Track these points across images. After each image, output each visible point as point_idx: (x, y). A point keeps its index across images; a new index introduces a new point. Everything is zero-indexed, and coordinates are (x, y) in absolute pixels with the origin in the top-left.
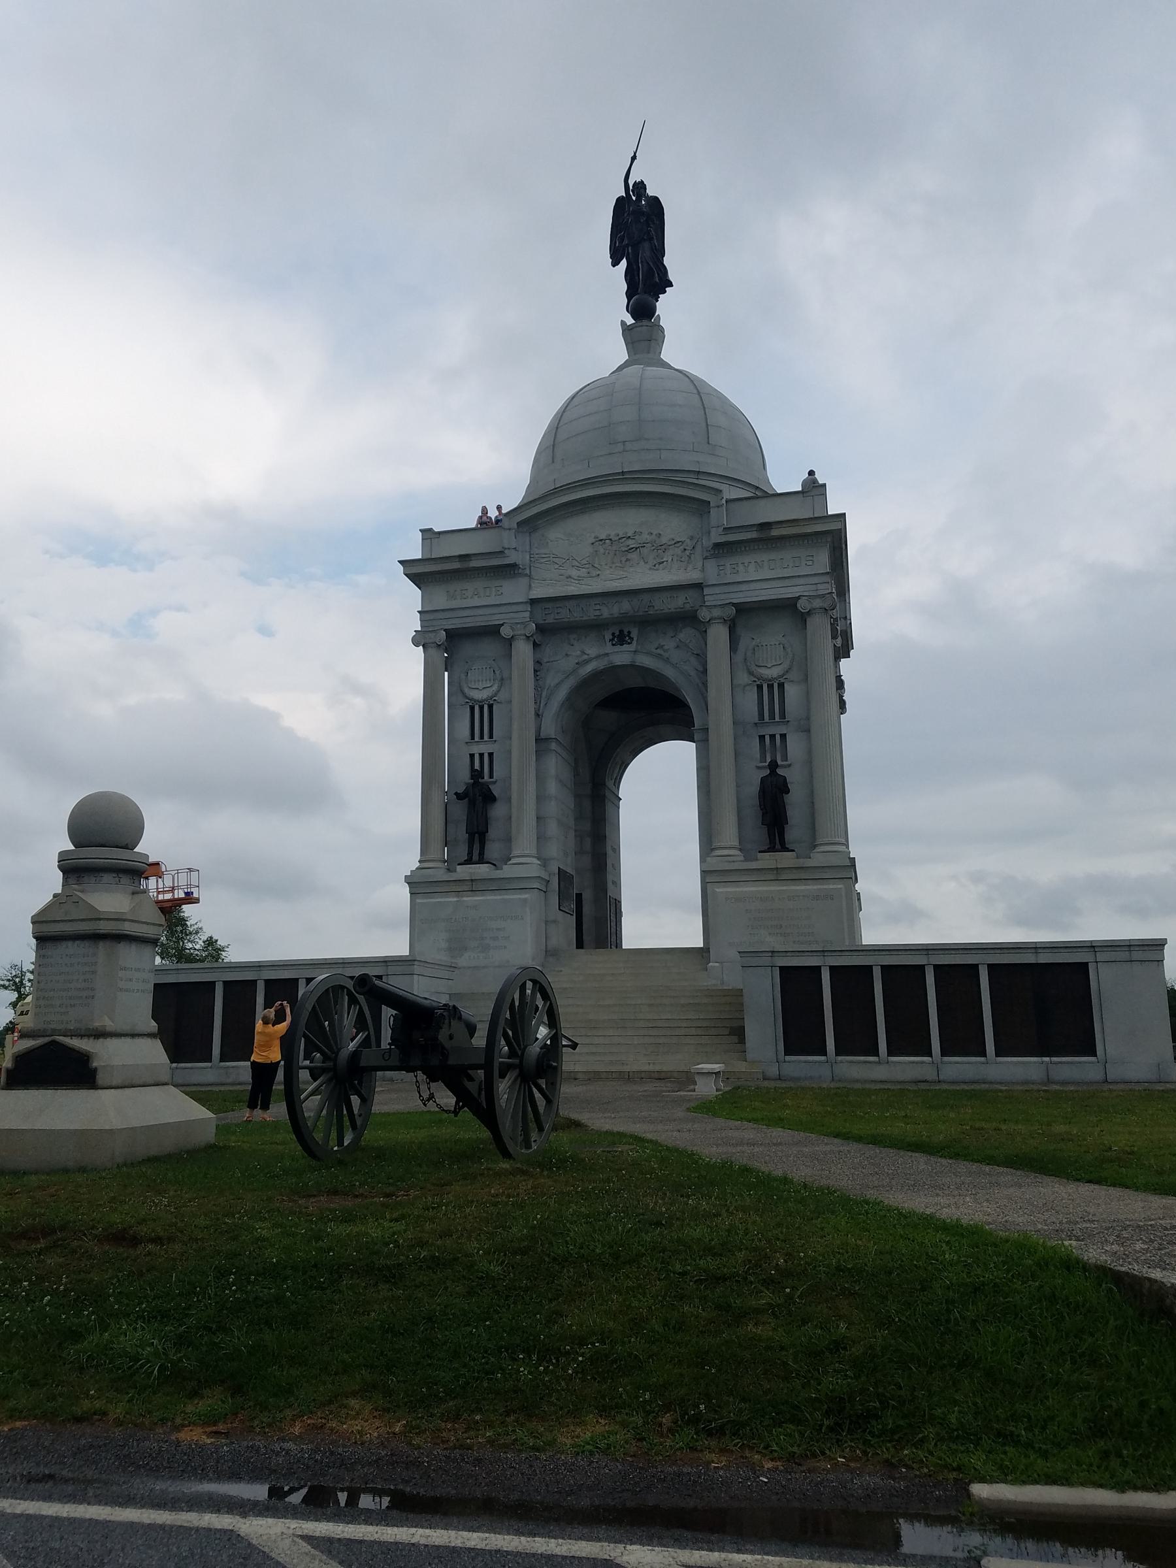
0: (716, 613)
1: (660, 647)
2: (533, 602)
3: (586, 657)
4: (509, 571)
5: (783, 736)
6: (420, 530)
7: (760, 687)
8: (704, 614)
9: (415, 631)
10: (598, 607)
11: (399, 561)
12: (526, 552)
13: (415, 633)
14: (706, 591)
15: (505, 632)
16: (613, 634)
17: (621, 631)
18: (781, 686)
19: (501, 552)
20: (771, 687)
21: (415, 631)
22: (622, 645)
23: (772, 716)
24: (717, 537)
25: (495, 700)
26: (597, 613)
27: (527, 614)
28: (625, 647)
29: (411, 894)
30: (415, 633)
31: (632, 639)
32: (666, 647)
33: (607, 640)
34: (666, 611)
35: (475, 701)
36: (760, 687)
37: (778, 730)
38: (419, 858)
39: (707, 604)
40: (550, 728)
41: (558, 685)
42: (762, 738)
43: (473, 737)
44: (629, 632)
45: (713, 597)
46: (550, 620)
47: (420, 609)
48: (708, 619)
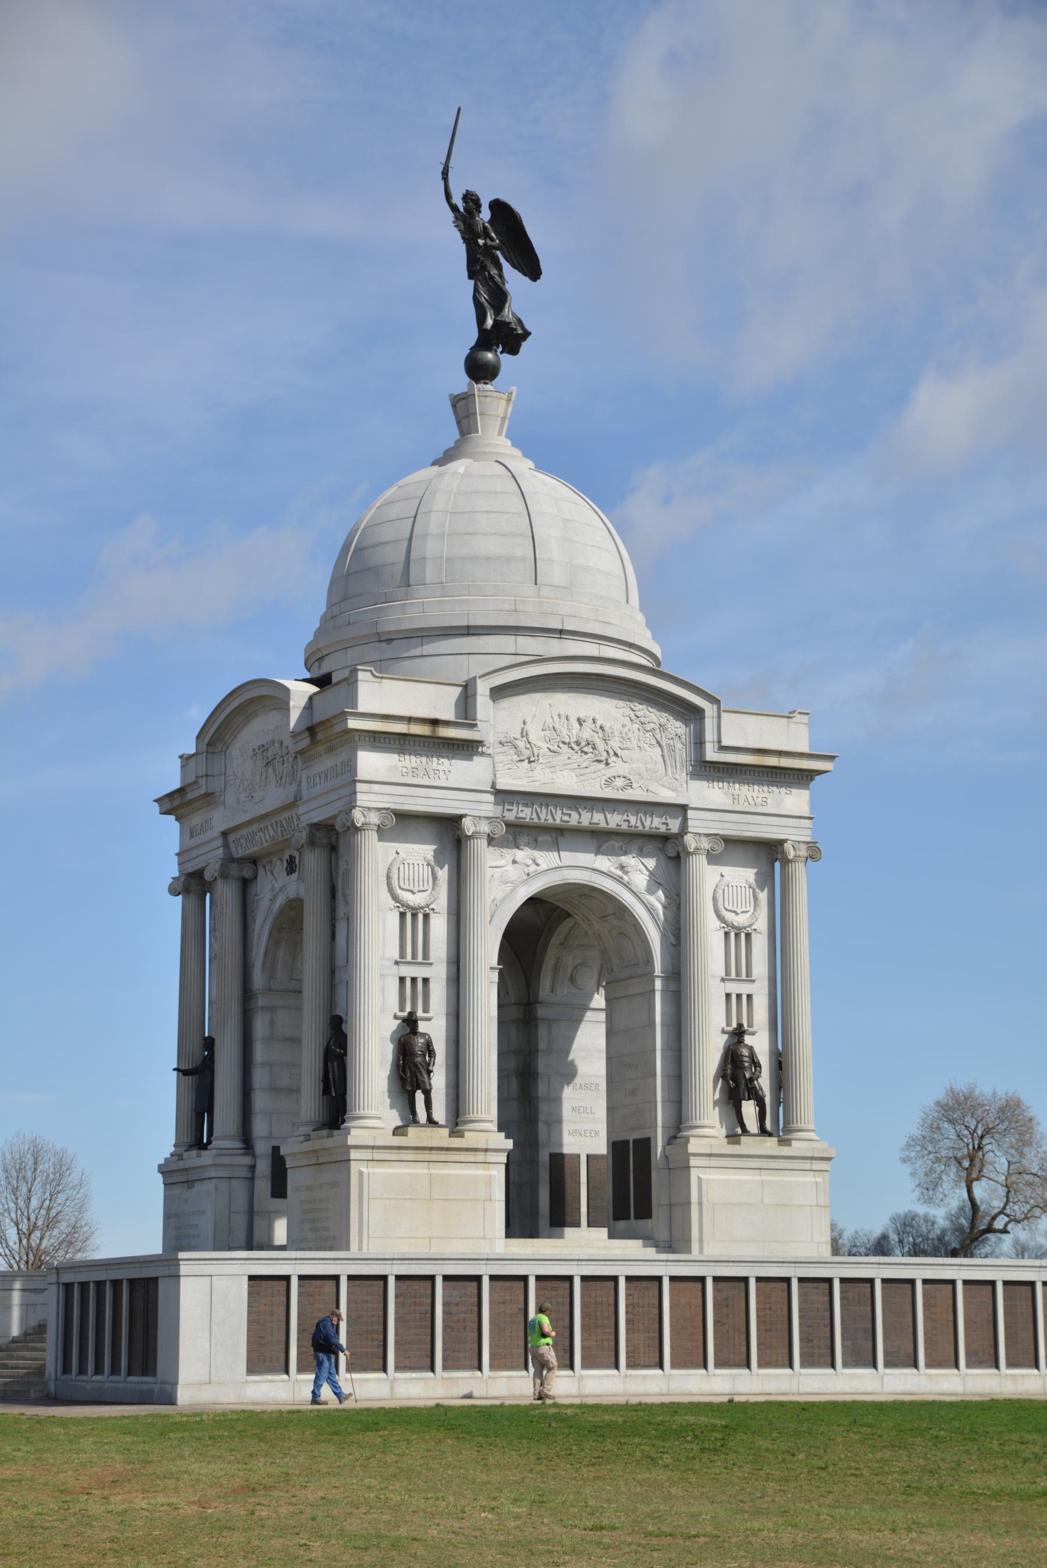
2: (225, 834)
4: (209, 799)
9: (172, 878)
11: (155, 801)
12: (221, 775)
14: (302, 809)
16: (287, 860)
17: (291, 856)
19: (196, 782)
21: (172, 878)
22: (291, 874)
27: (221, 850)
28: (295, 876)
29: (166, 1184)
30: (172, 880)
31: (296, 865)
33: (284, 869)
38: (173, 1141)
44: (295, 858)
47: (178, 851)
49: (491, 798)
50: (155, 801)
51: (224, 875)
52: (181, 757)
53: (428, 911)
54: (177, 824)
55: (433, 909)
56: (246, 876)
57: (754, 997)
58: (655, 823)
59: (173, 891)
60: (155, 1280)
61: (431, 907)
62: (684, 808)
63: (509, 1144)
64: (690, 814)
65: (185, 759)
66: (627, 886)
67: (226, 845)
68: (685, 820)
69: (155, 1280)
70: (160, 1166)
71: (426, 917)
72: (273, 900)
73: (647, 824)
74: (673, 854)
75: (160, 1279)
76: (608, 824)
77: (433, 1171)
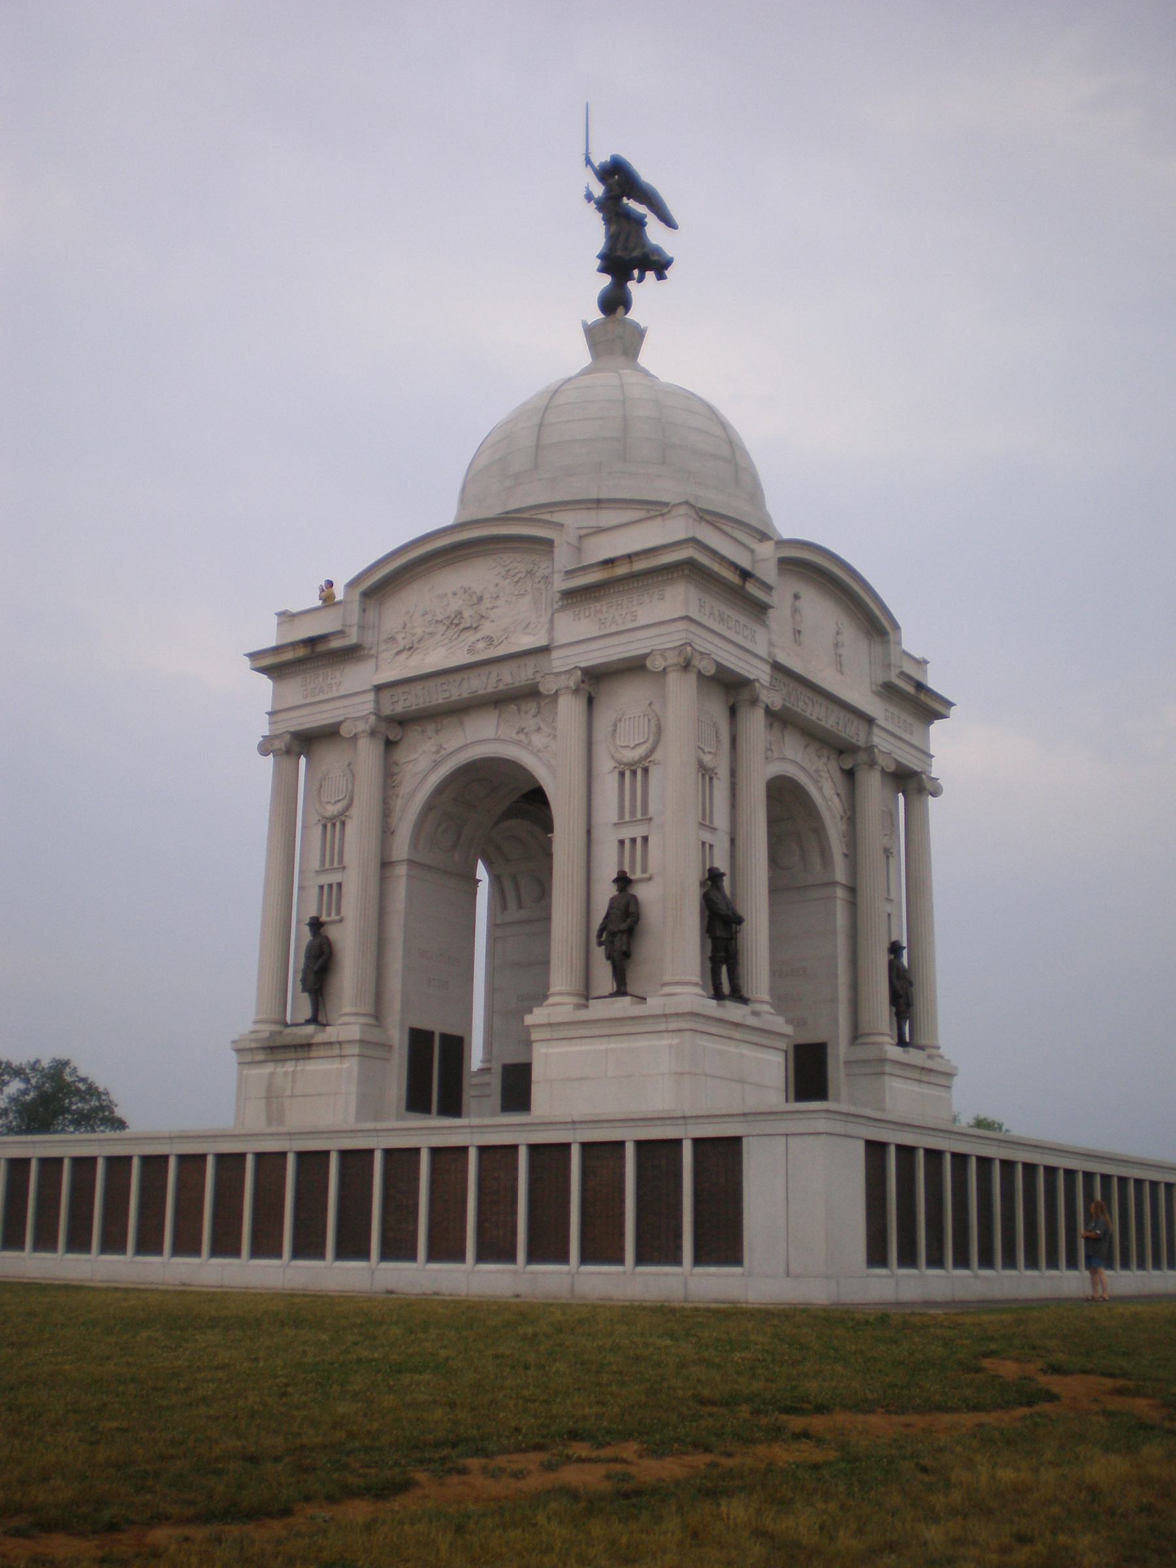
0: (562, 682)
1: (521, 731)
2: (379, 689)
3: (443, 752)
4: (351, 654)
5: (645, 839)
6: (276, 614)
7: (622, 774)
8: (548, 687)
9: (262, 737)
10: (445, 687)
11: (246, 655)
13: (262, 739)
14: (555, 654)
15: (344, 731)
18: (646, 770)
20: (634, 773)
21: (262, 737)
23: (633, 813)
24: (560, 584)
25: (346, 816)
26: (447, 695)
30: (262, 739)
32: (525, 731)
34: (517, 684)
35: (327, 818)
36: (622, 774)
37: (638, 831)
39: (555, 670)
40: (401, 848)
41: (414, 791)
42: (622, 842)
43: (324, 866)
45: (560, 661)
46: (399, 708)
47: (269, 710)
48: (554, 691)
49: (767, 669)
50: (246, 655)
51: (373, 733)
52: (281, 615)
53: (713, 775)
54: (270, 683)
55: (716, 774)
56: (391, 738)
57: (892, 917)
58: (853, 732)
59: (264, 750)
60: (734, 1143)
61: (715, 771)
62: (870, 721)
63: (789, 1030)
64: (876, 730)
65: (286, 617)
66: (820, 789)
67: (377, 702)
68: (870, 733)
69: (734, 1143)
70: (233, 1042)
71: (711, 779)
72: (436, 765)
73: (848, 730)
74: (847, 767)
75: (745, 1140)
76: (827, 723)
77: (745, 1052)
